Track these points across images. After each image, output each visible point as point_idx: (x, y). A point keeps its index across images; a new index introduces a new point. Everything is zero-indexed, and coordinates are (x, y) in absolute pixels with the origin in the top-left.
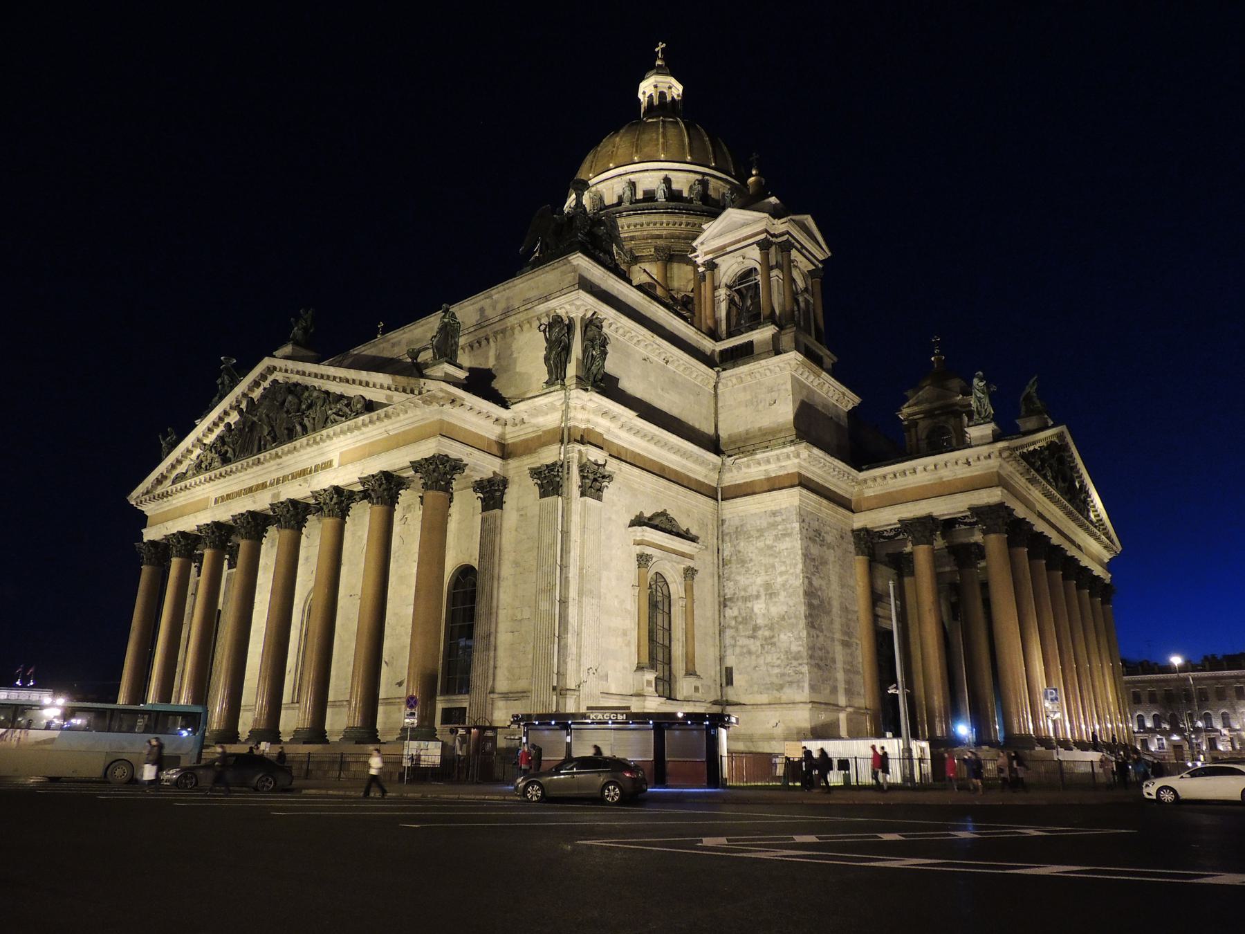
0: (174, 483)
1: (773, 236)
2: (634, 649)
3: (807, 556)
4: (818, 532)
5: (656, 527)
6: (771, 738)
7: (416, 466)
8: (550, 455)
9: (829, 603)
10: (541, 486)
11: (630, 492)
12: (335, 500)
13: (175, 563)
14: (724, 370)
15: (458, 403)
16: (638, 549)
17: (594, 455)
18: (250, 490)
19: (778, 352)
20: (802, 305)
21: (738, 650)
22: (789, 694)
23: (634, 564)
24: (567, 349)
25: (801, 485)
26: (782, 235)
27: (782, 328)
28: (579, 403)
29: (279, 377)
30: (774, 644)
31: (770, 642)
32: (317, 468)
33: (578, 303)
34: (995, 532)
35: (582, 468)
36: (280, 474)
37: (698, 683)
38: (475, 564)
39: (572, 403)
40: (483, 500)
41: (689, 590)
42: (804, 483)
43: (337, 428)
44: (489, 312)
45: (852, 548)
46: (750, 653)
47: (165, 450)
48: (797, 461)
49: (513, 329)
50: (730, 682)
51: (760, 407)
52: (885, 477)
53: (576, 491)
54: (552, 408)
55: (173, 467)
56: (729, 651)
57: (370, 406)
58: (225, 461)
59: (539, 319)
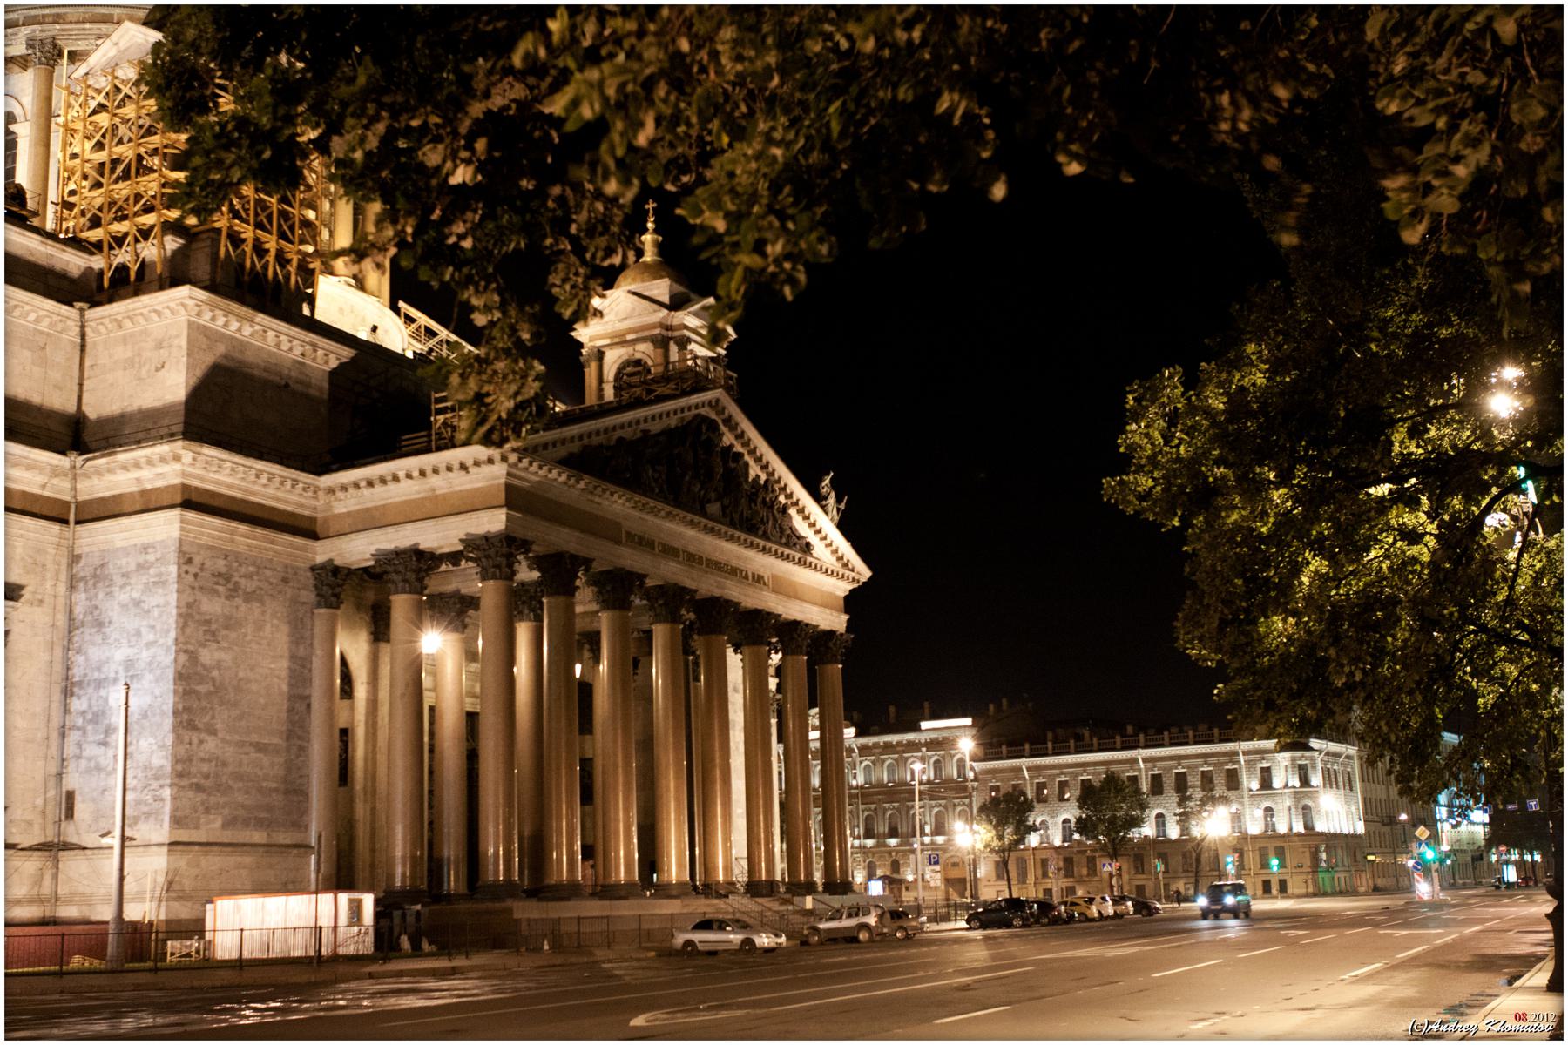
21: (83, 763)
48: (178, 466)
50: (70, 813)
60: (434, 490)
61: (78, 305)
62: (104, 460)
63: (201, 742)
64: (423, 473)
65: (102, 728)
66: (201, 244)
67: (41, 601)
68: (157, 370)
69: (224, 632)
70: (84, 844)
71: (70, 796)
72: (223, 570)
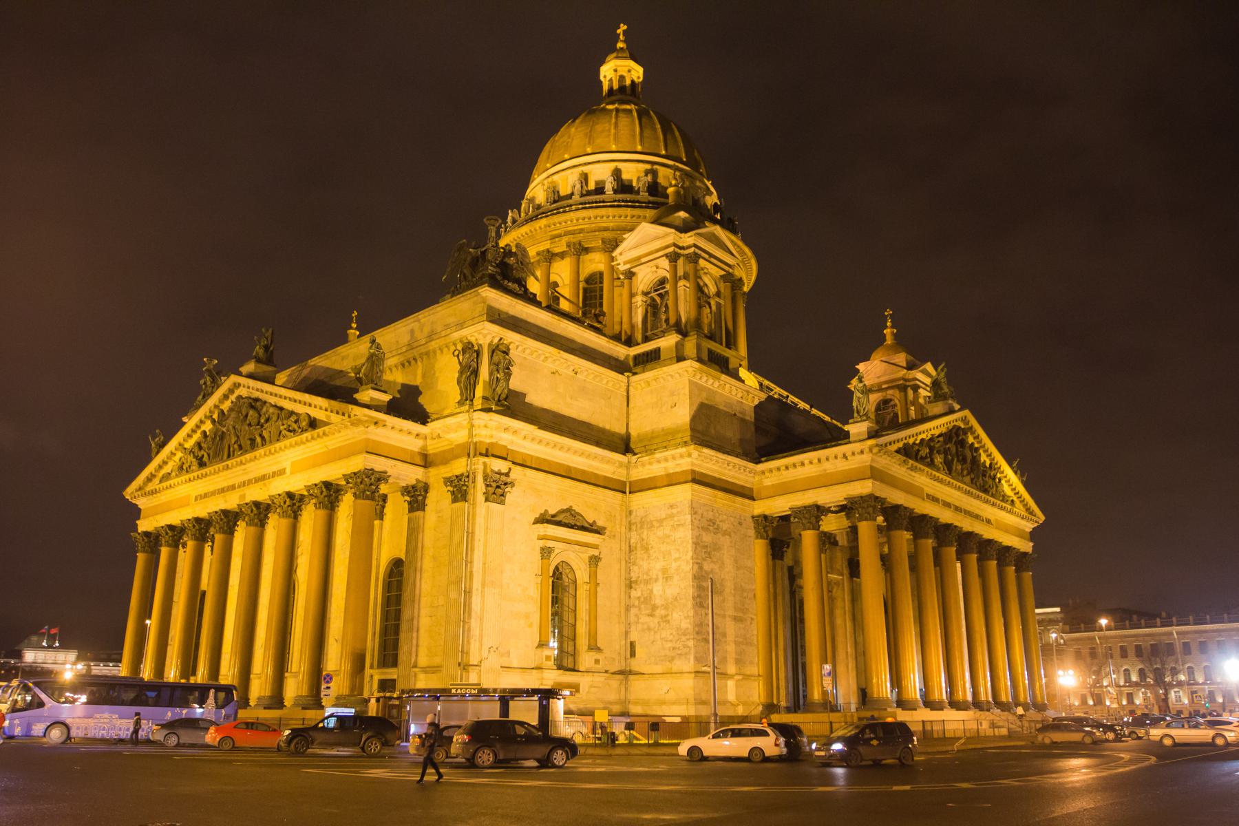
0: (161, 481)
1: (681, 248)
2: (536, 628)
3: (697, 544)
4: (712, 522)
5: (559, 524)
6: (662, 703)
7: (347, 478)
8: (459, 467)
9: (722, 585)
10: (453, 493)
11: (532, 493)
12: (288, 503)
13: (165, 551)
14: (635, 374)
15: (381, 424)
16: (542, 543)
18: (222, 490)
19: (680, 358)
20: (714, 308)
21: (640, 626)
22: (679, 665)
23: (537, 555)
24: (476, 373)
25: (694, 481)
26: (689, 247)
27: (685, 334)
28: (482, 423)
29: (243, 392)
30: (668, 622)
31: (665, 619)
32: (275, 474)
33: (485, 332)
34: (866, 519)
35: (486, 477)
36: (245, 478)
37: (598, 656)
38: (403, 557)
39: (476, 422)
40: (410, 503)
41: (593, 575)
42: (699, 479)
43: (287, 442)
44: (418, 334)
45: (752, 532)
46: (649, 629)
47: (154, 450)
48: (689, 460)
49: (435, 352)
50: (633, 654)
52: (779, 469)
53: (480, 497)
54: (460, 426)
55: (160, 467)
56: (633, 628)
57: (313, 424)
58: (202, 464)
59: (455, 344)
64: (819, 460)
71: (632, 645)
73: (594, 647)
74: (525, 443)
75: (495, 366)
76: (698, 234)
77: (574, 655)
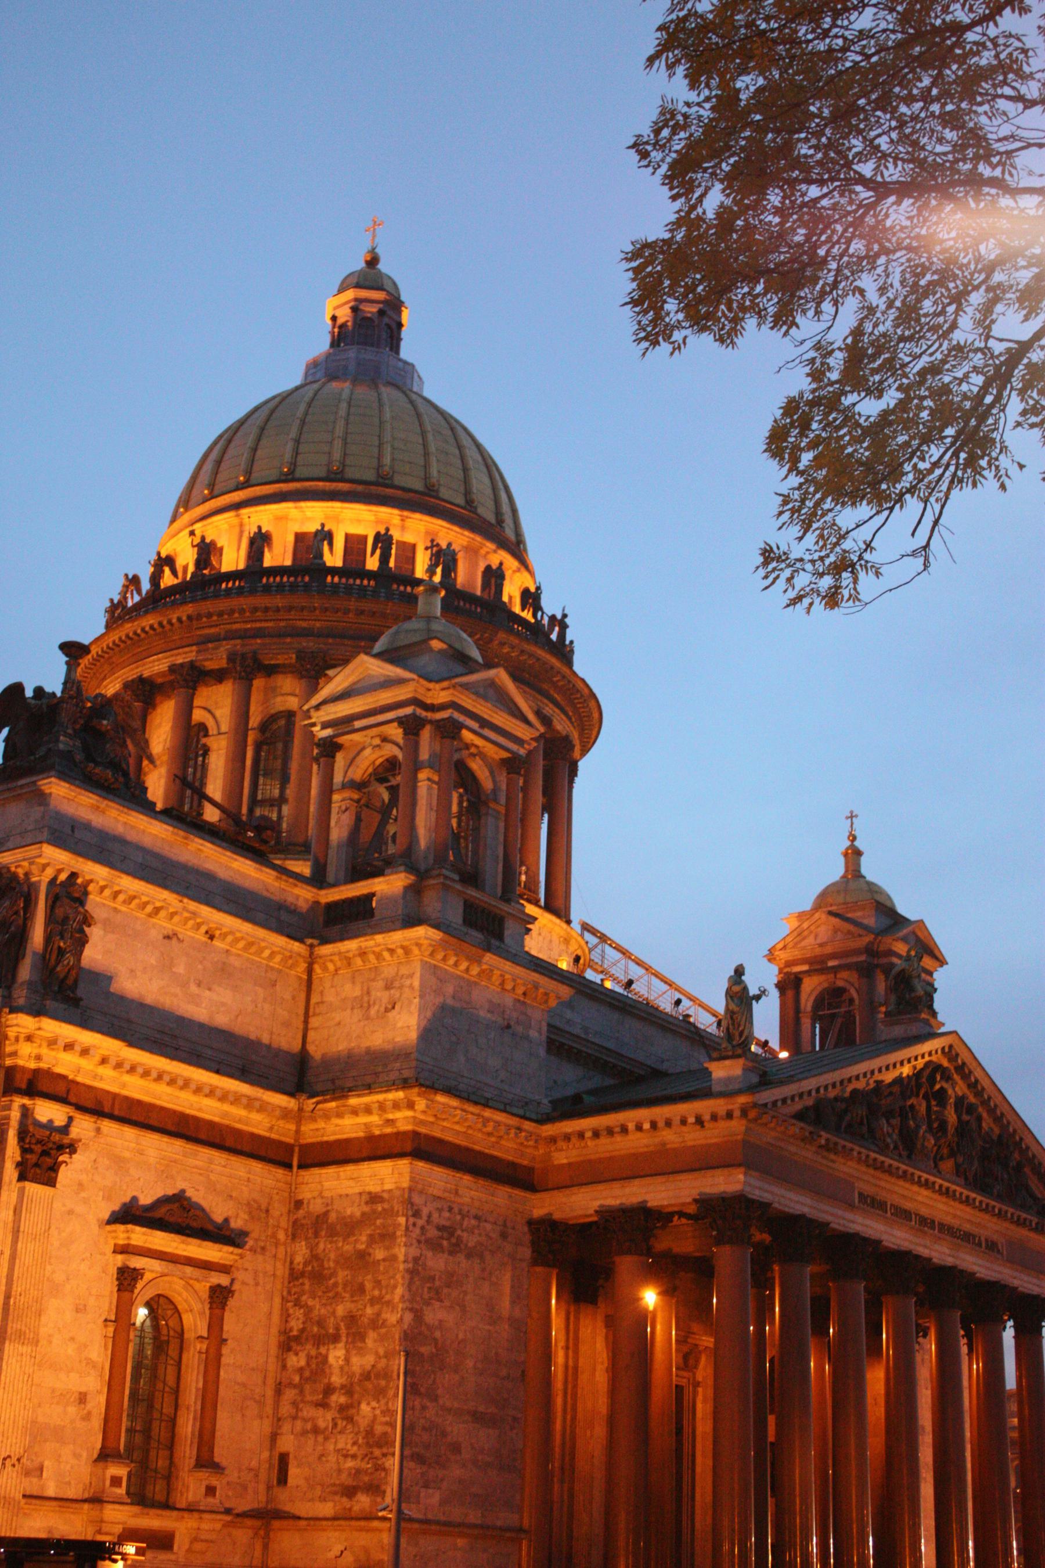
11: (111, 1165)
17: (48, 1112)
21: (299, 1424)
23: (109, 1286)
30: (350, 1419)
41: (216, 1324)
46: (316, 1430)
48: (409, 1113)
50: (283, 1479)
51: (373, 1012)
56: (286, 1427)
60: (664, 1144)
61: (309, 941)
62: (333, 1104)
63: (424, 1408)
64: (654, 1125)
65: (320, 1387)
66: (432, 882)
67: (263, 1248)
68: (387, 1010)
69: (445, 1290)
70: (297, 1513)
71: (283, 1460)
72: (447, 1224)
73: (206, 1462)
74: (106, 1071)
75: (56, 925)
76: (463, 686)
77: (169, 1477)
